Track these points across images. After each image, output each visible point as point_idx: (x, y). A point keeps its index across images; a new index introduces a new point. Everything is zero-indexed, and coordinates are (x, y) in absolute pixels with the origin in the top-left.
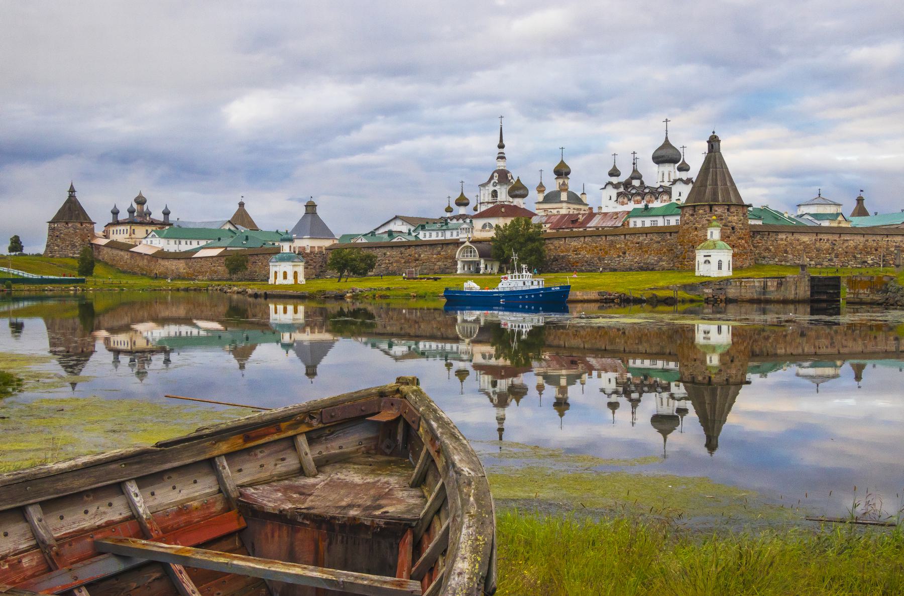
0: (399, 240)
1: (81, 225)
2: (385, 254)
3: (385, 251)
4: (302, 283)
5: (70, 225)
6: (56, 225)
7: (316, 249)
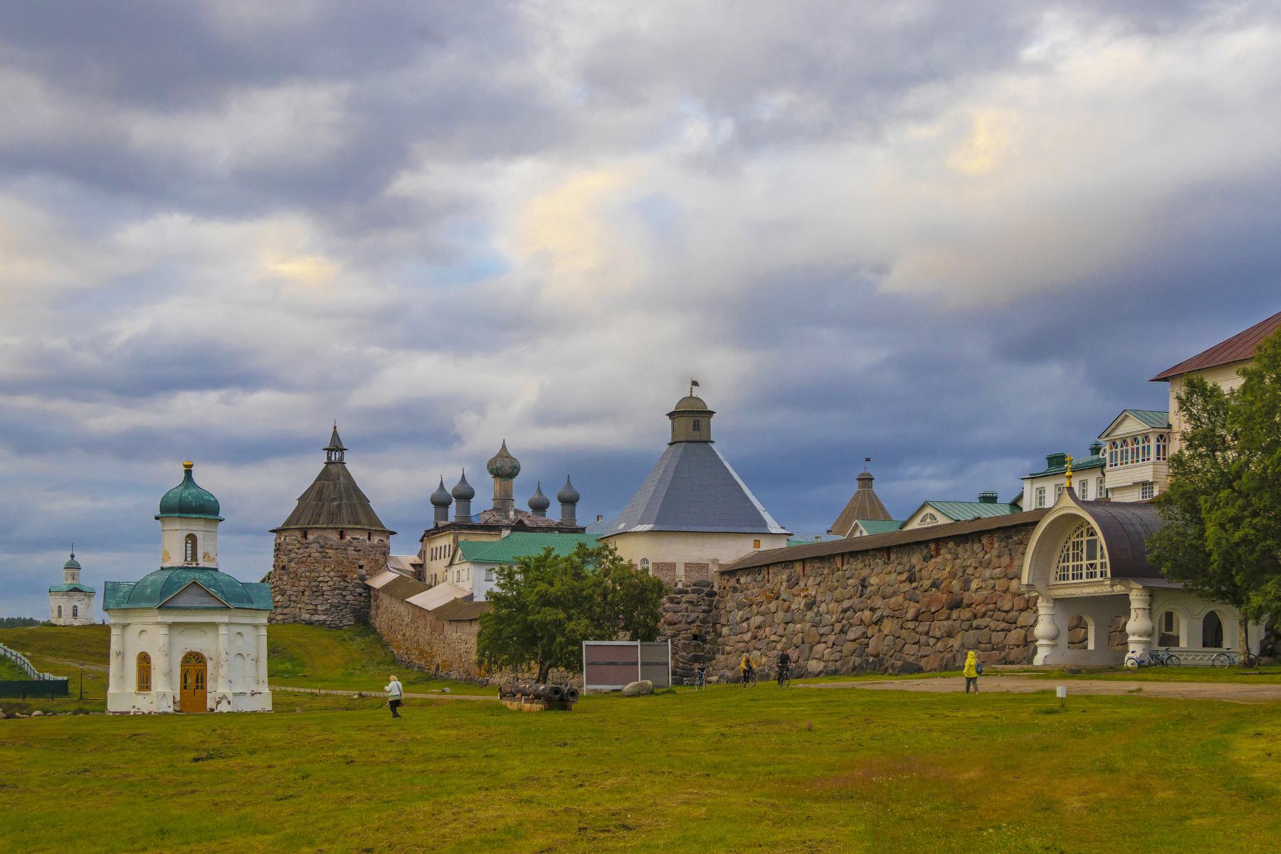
0: (929, 523)
1: (342, 537)
2: (864, 584)
3: (866, 572)
4: (247, 705)
5: (311, 537)
6: (282, 539)
7: (680, 571)
